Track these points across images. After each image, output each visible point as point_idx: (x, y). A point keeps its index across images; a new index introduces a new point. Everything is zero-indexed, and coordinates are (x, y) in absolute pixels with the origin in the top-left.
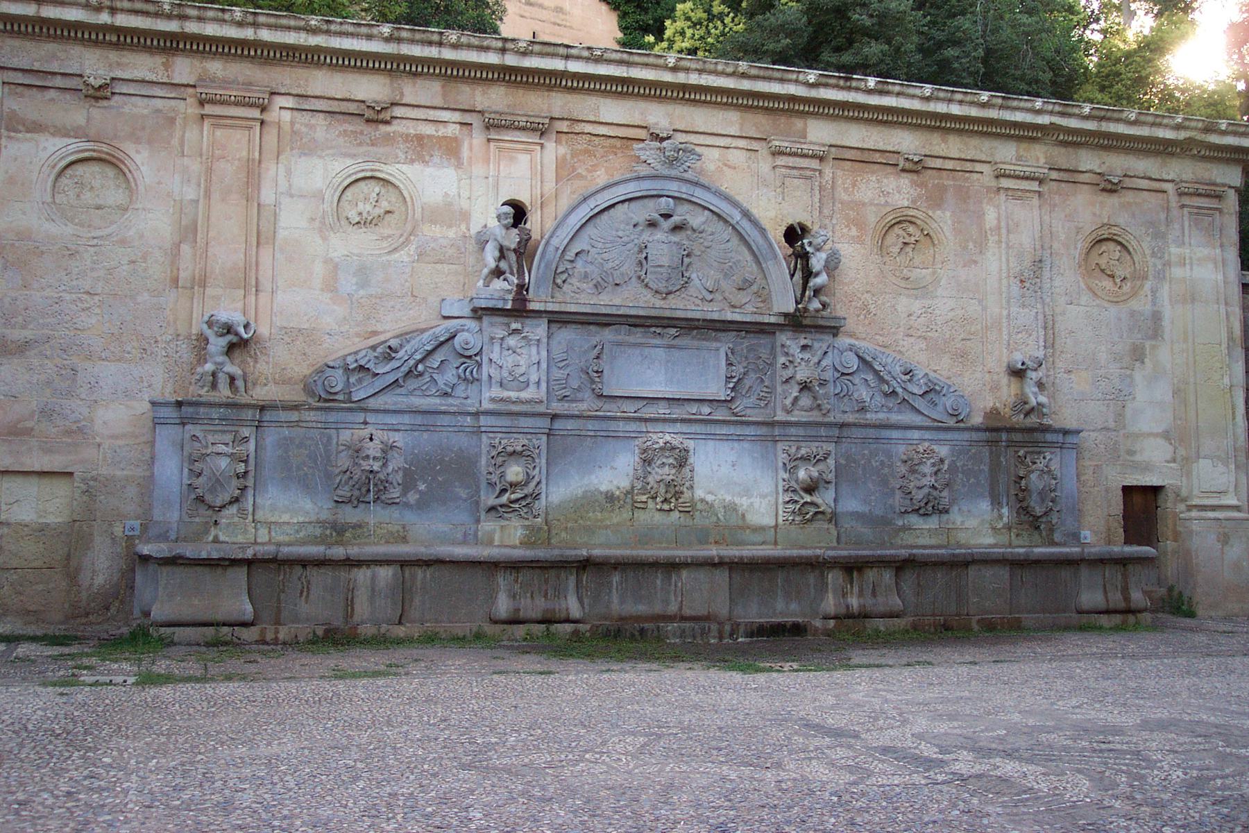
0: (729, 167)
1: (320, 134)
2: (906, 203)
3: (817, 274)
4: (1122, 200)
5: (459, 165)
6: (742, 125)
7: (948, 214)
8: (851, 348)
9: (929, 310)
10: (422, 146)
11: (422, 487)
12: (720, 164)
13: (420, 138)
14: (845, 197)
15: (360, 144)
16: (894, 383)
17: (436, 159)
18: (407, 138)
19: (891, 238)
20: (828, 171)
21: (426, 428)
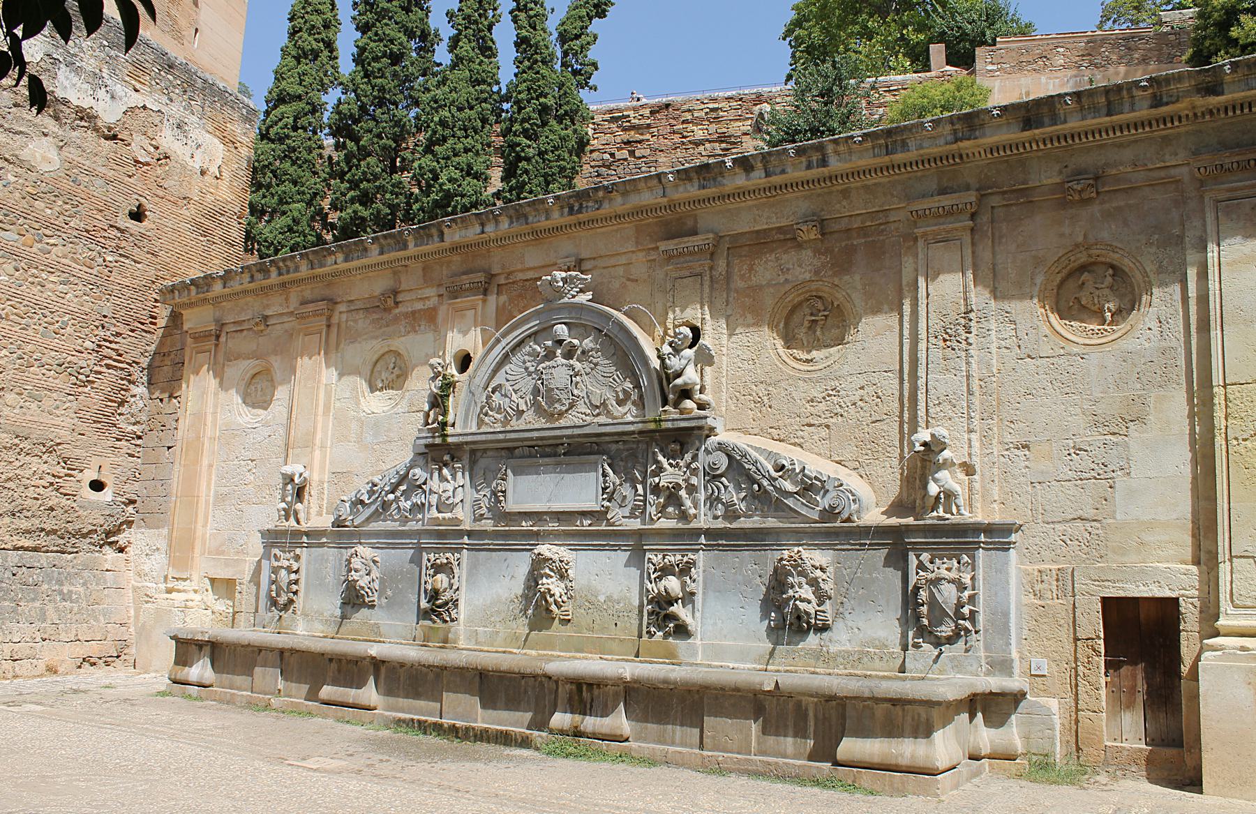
0: (632, 280)
1: (361, 324)
2: (807, 276)
3: (679, 375)
4: (1107, 206)
5: (436, 331)
6: (637, 238)
7: (857, 277)
8: (721, 447)
9: (834, 393)
10: (414, 319)
11: (389, 593)
12: (624, 280)
13: (414, 313)
14: (740, 284)
15: (380, 328)
16: (765, 483)
17: (422, 327)
18: (406, 315)
19: (796, 318)
20: (722, 264)
21: (394, 547)
